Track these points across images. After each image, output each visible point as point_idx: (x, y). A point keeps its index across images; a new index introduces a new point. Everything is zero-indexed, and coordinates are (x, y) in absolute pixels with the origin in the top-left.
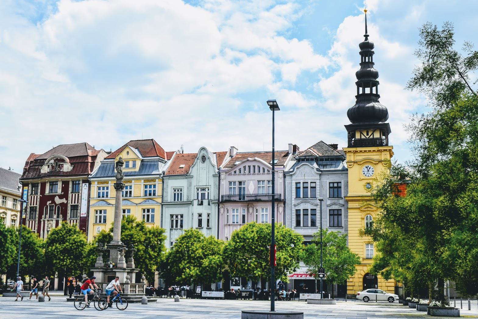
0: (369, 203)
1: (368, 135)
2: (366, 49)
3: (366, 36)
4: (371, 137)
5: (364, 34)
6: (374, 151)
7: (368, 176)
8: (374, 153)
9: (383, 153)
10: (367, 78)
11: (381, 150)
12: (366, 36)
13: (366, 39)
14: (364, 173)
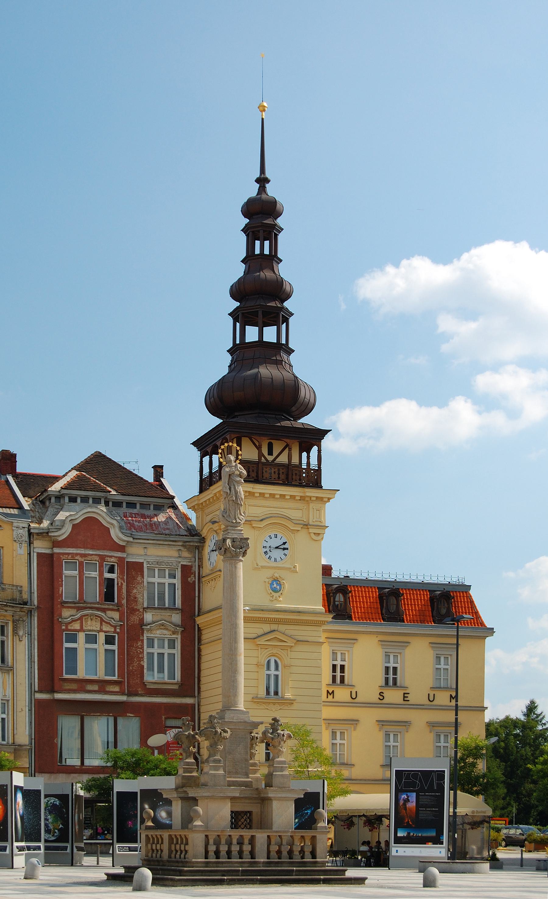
0: (276, 629)
1: (270, 453)
2: (261, 218)
3: (262, 181)
4: (279, 460)
5: (258, 175)
6: (293, 497)
7: (275, 560)
8: (292, 504)
9: (311, 505)
10: (260, 297)
11: (310, 497)
12: (262, 181)
13: (262, 189)
14: (266, 553)
